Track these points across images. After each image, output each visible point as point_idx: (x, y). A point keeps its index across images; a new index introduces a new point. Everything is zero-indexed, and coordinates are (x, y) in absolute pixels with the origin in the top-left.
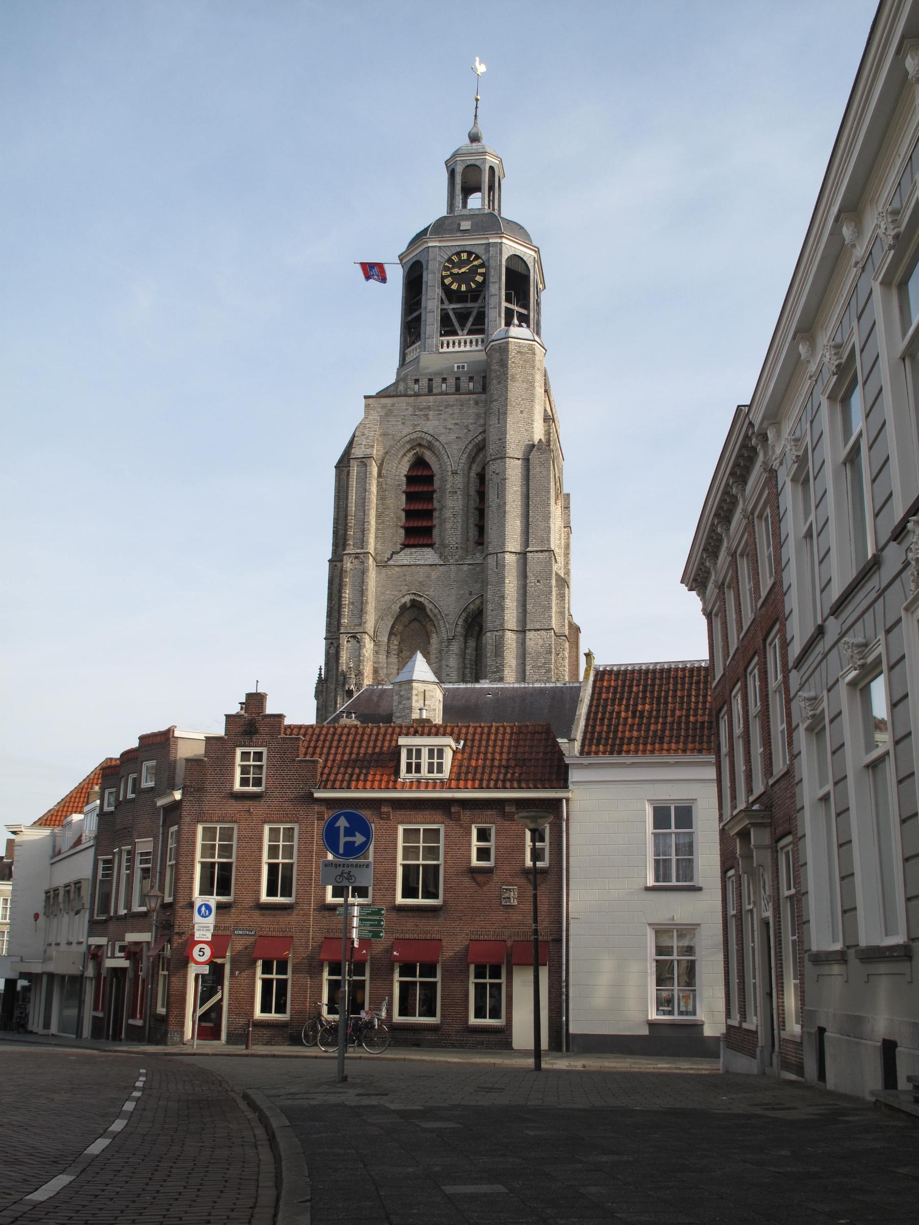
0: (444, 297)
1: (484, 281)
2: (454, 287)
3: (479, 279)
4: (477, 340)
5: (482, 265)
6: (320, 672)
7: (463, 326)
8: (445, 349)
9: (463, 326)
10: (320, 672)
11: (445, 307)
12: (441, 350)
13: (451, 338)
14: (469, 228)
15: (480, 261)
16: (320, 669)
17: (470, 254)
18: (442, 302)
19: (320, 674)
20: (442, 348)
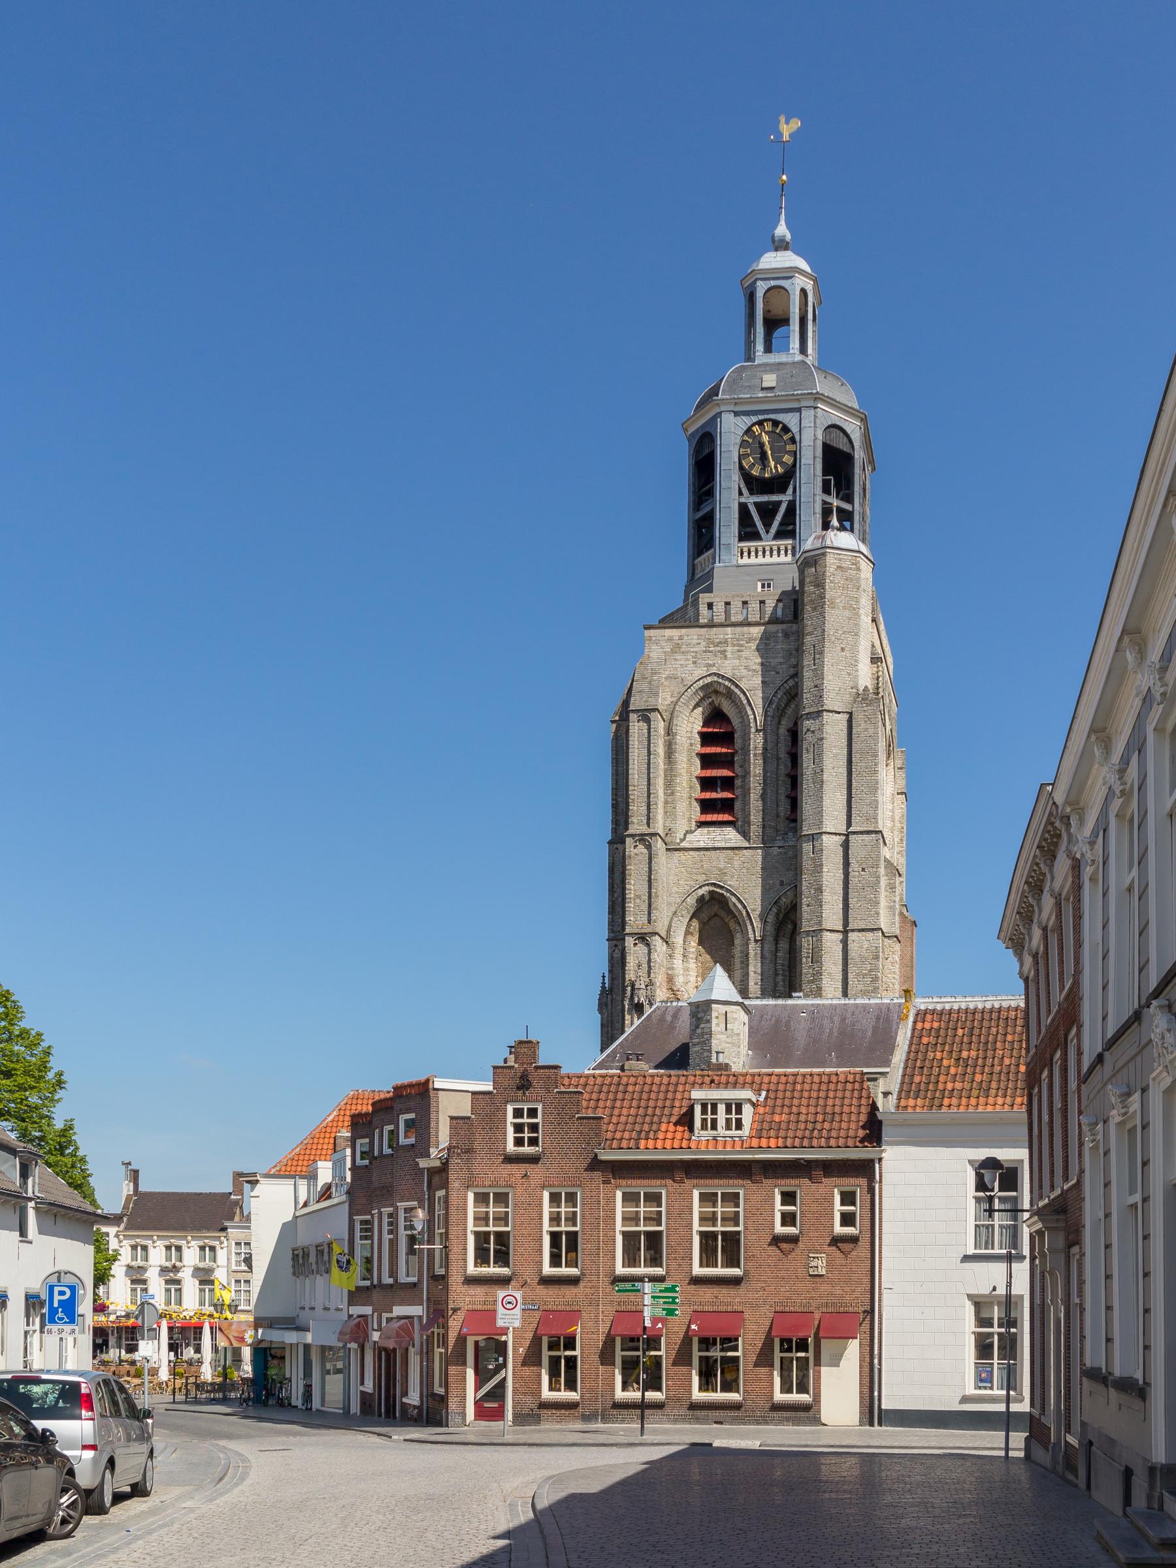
0: (743, 485)
2: (755, 472)
3: (788, 459)
6: (604, 980)
7: (767, 525)
9: (767, 525)
10: (604, 980)
11: (743, 500)
12: (741, 562)
14: (774, 384)
15: (789, 435)
16: (604, 977)
18: (741, 493)
19: (604, 983)
20: (742, 558)
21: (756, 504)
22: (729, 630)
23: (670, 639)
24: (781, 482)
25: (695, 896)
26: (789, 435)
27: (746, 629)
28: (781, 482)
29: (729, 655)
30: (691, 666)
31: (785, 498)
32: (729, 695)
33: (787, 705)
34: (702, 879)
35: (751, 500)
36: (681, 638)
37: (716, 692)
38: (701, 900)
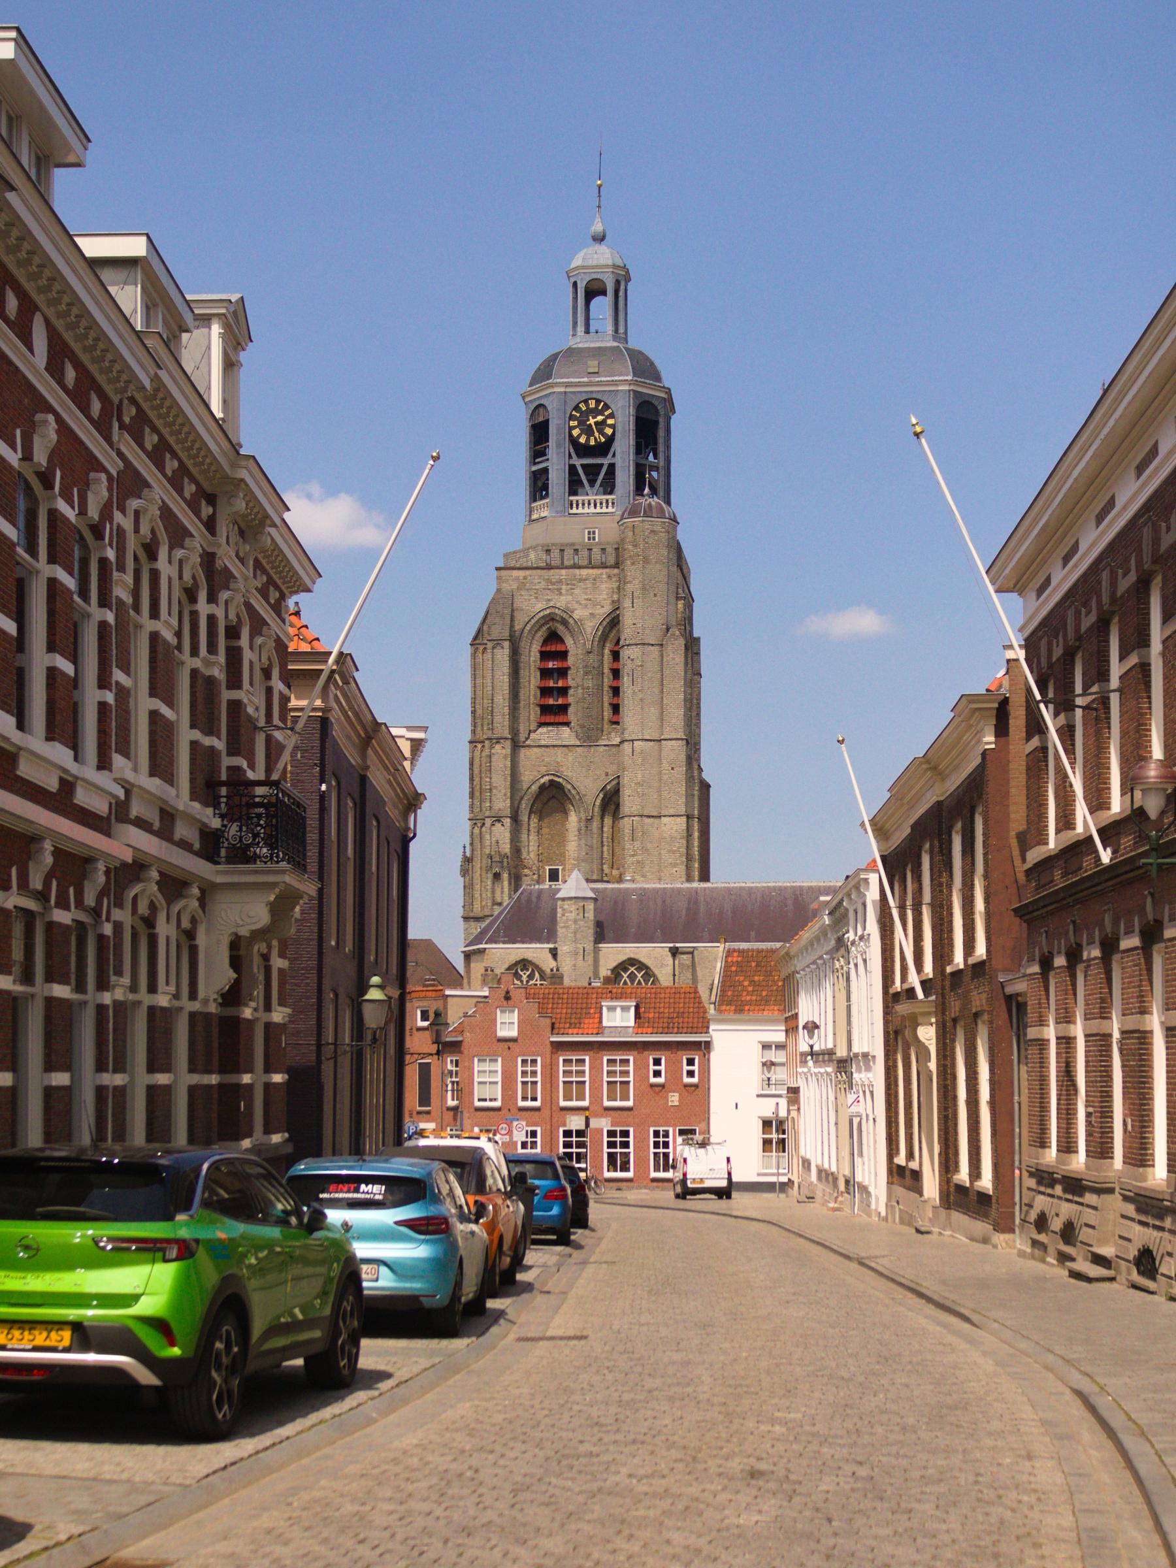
0: (572, 451)
1: (613, 434)
2: (582, 440)
3: (609, 431)
4: (607, 501)
5: (611, 416)
8: (574, 511)
11: (572, 462)
13: (579, 498)
17: (598, 401)
18: (570, 456)
21: (583, 466)
22: (563, 572)
23: (517, 578)
24: (604, 449)
25: (538, 784)
26: (609, 411)
27: (577, 571)
28: (604, 449)
29: (563, 592)
30: (533, 601)
31: (606, 461)
32: (564, 622)
33: (610, 631)
34: (543, 770)
35: (578, 462)
36: (525, 578)
37: (553, 619)
38: (543, 788)
